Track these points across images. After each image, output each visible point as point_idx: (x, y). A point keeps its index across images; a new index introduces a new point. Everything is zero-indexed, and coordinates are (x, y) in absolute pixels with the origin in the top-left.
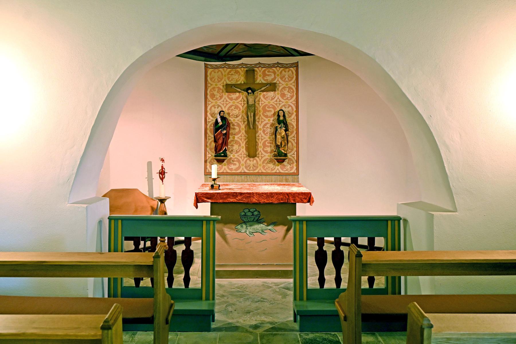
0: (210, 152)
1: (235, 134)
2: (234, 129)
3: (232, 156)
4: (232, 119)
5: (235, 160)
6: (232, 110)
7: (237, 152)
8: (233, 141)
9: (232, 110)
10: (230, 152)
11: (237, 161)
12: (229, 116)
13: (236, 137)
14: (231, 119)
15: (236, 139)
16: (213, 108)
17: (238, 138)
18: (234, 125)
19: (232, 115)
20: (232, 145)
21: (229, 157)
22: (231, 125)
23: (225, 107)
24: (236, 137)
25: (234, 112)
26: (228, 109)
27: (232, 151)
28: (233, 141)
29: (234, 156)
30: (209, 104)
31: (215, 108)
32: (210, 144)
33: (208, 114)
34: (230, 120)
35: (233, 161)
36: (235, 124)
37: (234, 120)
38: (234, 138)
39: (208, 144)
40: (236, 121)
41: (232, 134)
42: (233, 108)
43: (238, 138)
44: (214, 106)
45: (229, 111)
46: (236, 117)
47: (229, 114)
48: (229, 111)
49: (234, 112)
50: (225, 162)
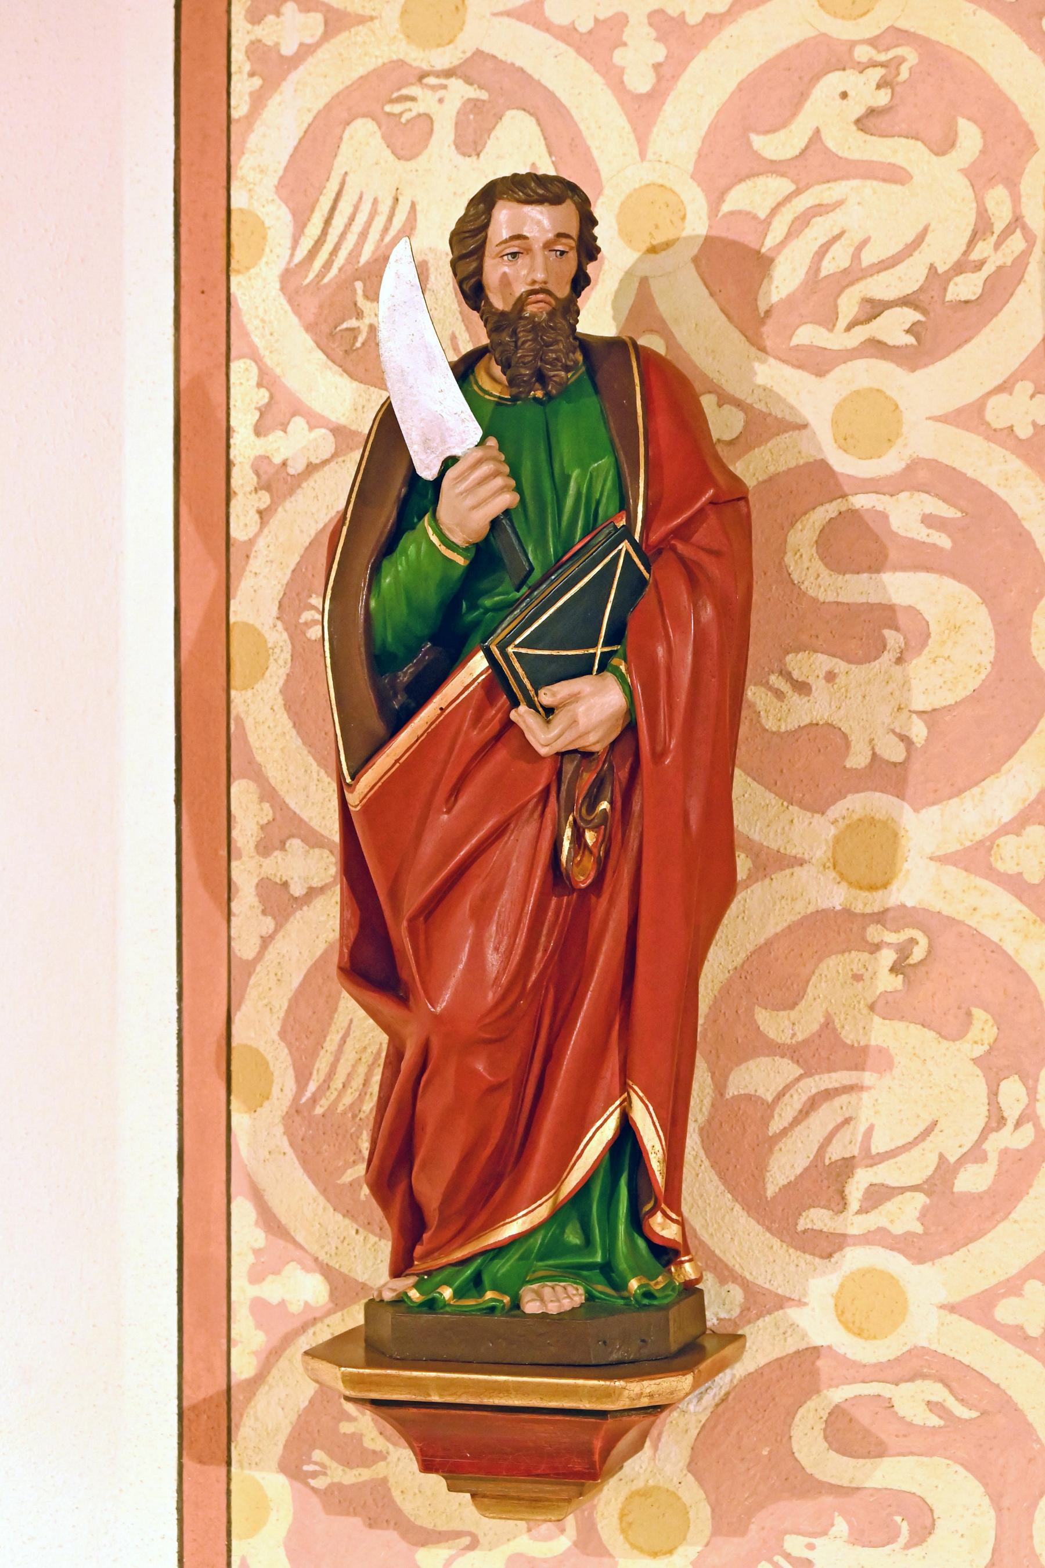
0: (296, 1193)
1: (889, 776)
2: (869, 633)
3: (815, 1321)
4: (813, 401)
5: (912, 1401)
6: (815, 163)
7: (951, 1219)
8: (836, 931)
9: (815, 163)
10: (779, 1215)
11: (939, 1440)
12: (751, 322)
13: (925, 830)
14: (800, 402)
15: (916, 885)
16: (362, 142)
17: (975, 858)
18: (856, 543)
19: (820, 293)
20: (829, 1051)
21: (762, 1347)
22: (798, 560)
23: (643, 110)
24: (925, 830)
25: (867, 217)
26: (726, 158)
27: (829, 1179)
28: (836, 931)
29: (870, 1306)
30: (275, 67)
31: (408, 139)
32: (303, 1031)
33: (258, 293)
34: (765, 424)
35: (847, 1433)
36: (906, 516)
37: (872, 420)
38: (870, 856)
39: (259, 1027)
40: (924, 440)
41: (818, 768)
42: (830, 109)
43: (975, 858)
44: (379, 96)
45: (753, 196)
46: (922, 350)
47: (733, 265)
48: (753, 196)
49: (867, 217)
50: (657, 1464)
